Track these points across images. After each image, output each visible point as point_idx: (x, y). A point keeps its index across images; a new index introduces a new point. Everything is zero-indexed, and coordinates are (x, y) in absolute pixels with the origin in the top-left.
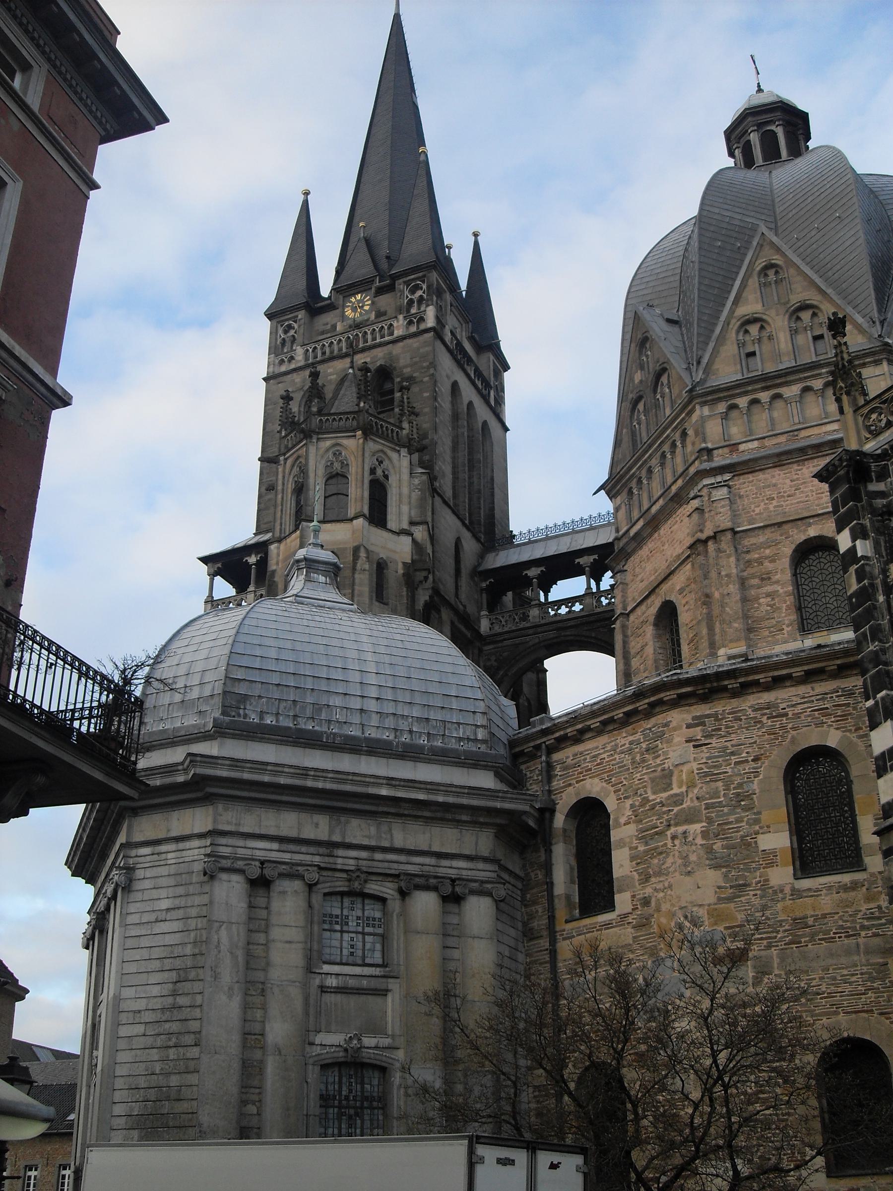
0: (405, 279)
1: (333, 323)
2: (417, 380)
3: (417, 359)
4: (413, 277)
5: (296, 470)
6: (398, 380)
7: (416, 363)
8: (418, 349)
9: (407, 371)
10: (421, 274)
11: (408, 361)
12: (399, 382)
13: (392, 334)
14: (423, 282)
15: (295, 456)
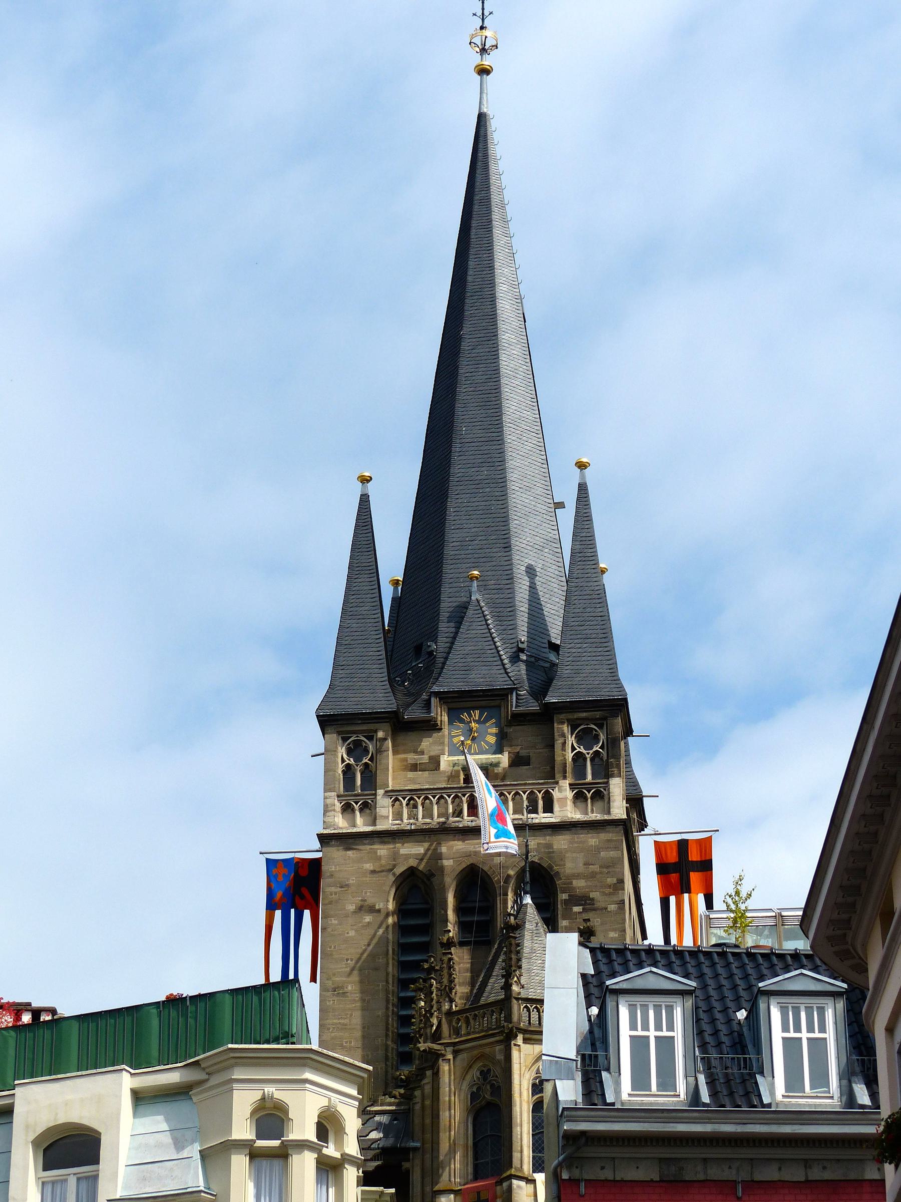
0: (570, 716)
1: (432, 753)
2: (597, 905)
3: (596, 868)
4: (584, 715)
5: (475, 1073)
6: (565, 896)
7: (593, 875)
8: (598, 849)
9: (579, 884)
10: (598, 714)
11: (581, 868)
12: (566, 902)
13: (549, 808)
14: (601, 726)
15: (475, 1052)
